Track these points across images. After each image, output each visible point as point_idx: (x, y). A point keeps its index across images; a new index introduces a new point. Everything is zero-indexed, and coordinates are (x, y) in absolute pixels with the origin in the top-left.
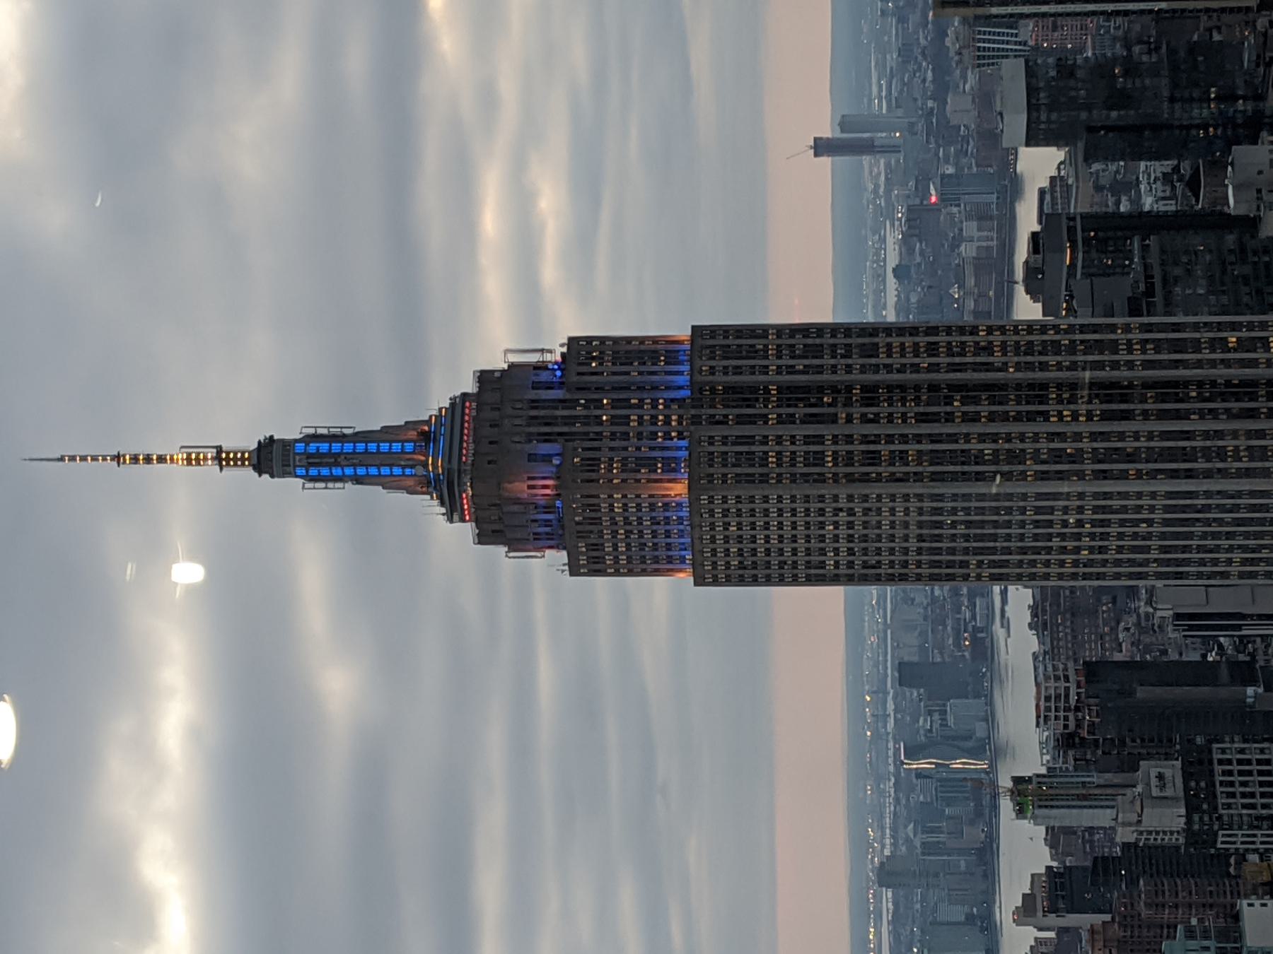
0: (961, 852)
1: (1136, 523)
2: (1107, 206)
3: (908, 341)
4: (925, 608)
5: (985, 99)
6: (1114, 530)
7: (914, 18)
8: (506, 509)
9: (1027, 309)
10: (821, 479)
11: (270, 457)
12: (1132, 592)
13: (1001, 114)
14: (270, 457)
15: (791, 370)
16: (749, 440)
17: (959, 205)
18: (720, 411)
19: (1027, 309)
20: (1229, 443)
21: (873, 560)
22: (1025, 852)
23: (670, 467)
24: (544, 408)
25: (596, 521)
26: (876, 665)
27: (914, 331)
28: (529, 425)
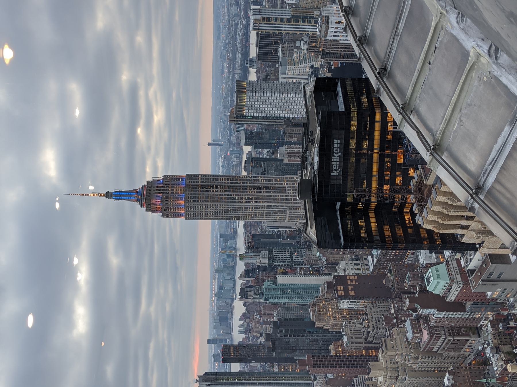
0: (230, 267)
1: (261, 211)
3: (224, 178)
5: (238, 137)
6: (258, 212)
7: (226, 123)
9: (244, 173)
10: (208, 202)
11: (108, 195)
12: (261, 222)
14: (108, 195)
15: (203, 182)
16: (195, 194)
18: (190, 189)
19: (244, 173)
20: (277, 197)
22: (241, 267)
23: (181, 198)
25: (168, 208)
27: (225, 176)
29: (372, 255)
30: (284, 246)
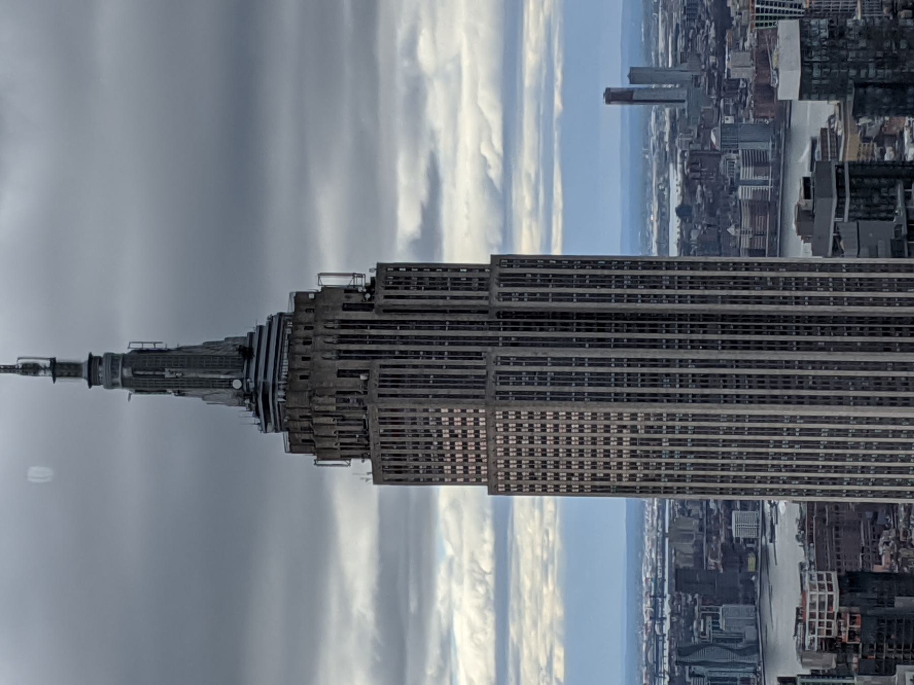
2: (873, 155)
4: (701, 520)
8: (315, 420)
13: (777, 70)
17: (737, 152)
21: (652, 473)
24: (354, 328)
26: (655, 570)
28: (341, 342)
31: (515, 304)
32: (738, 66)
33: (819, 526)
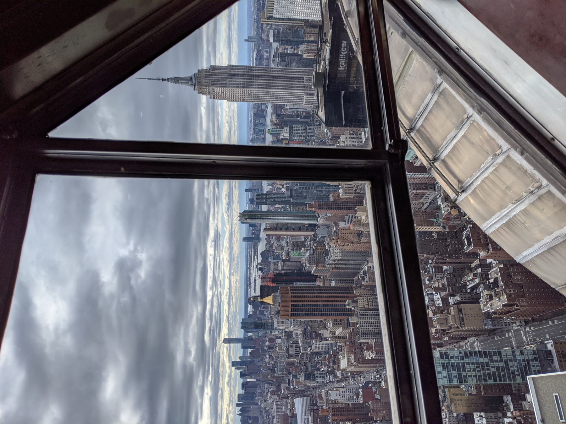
9: (273, 66)
29: (365, 132)
30: (301, 123)
31: (231, 72)
32: (264, 37)
33: (275, 107)
